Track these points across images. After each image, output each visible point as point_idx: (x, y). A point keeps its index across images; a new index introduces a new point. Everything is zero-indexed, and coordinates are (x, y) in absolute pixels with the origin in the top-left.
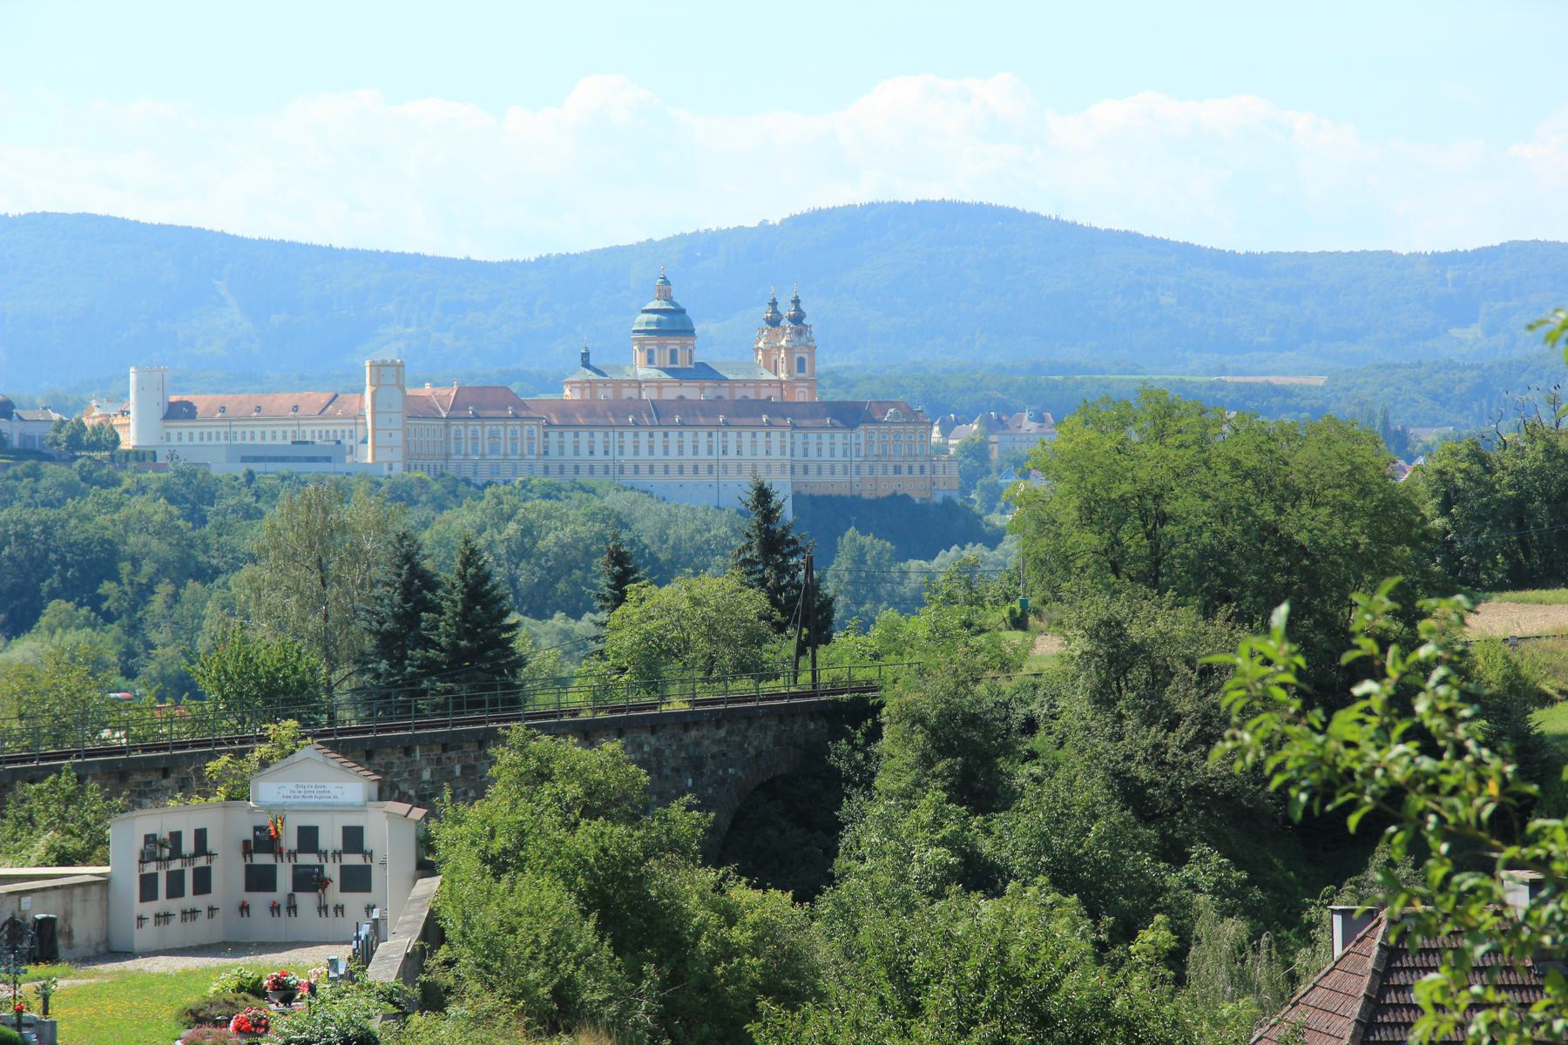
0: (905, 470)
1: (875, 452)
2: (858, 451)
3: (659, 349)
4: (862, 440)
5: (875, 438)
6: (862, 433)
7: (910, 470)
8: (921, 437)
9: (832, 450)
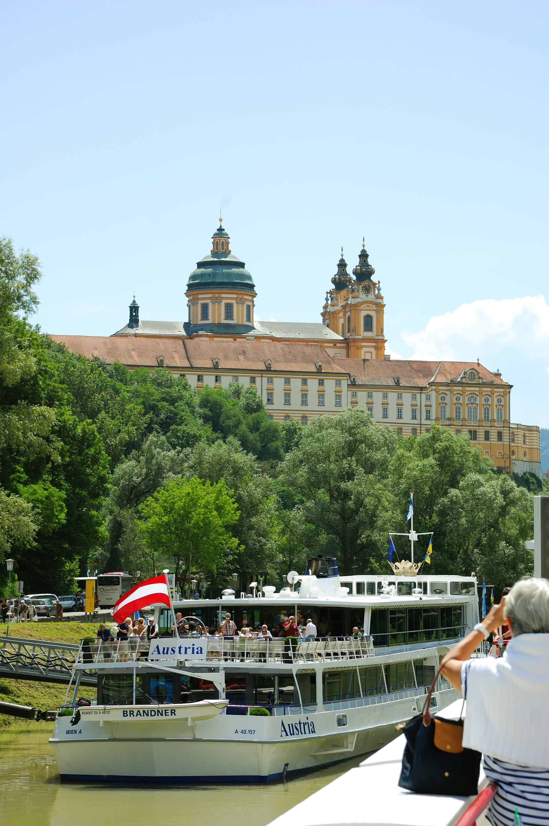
0: (481, 435)
1: (448, 415)
2: (428, 412)
3: (237, 303)
4: (433, 402)
5: (448, 400)
6: (433, 394)
7: (487, 437)
8: (499, 401)
9: (400, 412)
